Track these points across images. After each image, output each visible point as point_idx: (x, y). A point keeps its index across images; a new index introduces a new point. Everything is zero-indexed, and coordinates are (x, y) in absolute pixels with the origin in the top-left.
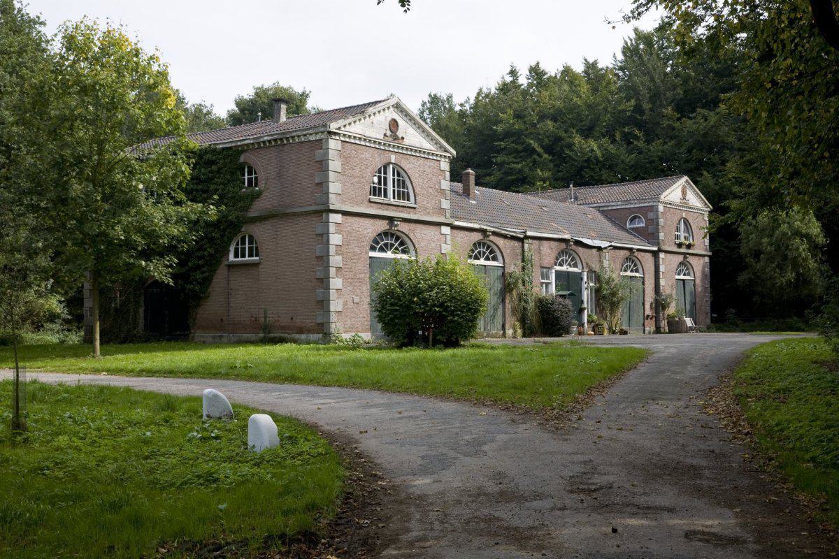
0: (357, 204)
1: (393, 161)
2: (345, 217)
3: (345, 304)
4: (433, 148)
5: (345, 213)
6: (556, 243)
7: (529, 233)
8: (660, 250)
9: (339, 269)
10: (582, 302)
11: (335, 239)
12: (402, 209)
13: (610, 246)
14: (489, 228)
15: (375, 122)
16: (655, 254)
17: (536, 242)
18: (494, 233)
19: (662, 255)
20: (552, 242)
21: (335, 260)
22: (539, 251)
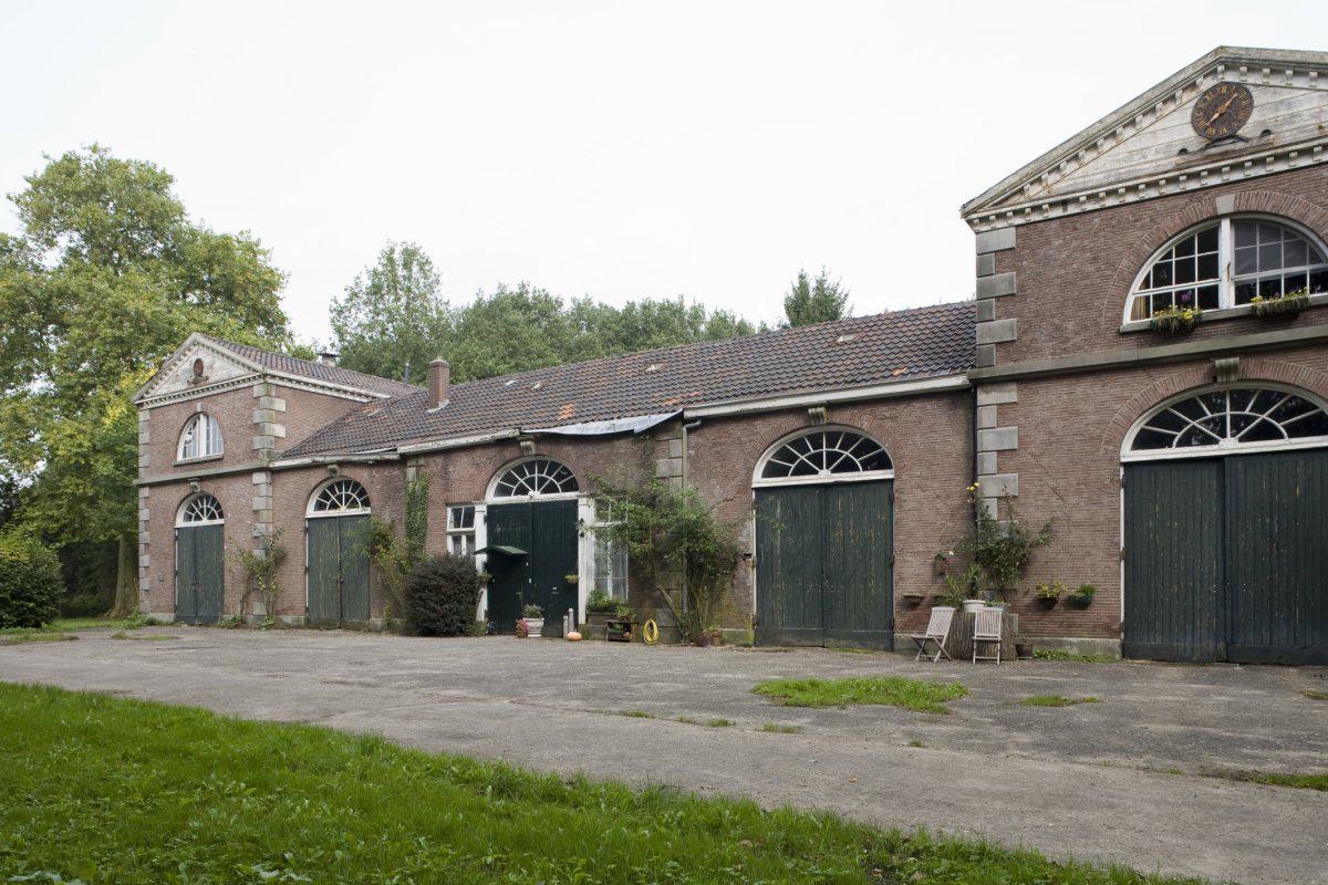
0: (163, 472)
1: (199, 410)
2: (154, 490)
3: (151, 582)
4: (243, 372)
5: (152, 485)
6: (492, 452)
7: (402, 449)
8: (977, 384)
9: (147, 545)
10: (572, 565)
11: (144, 514)
12: (190, 467)
13: (680, 418)
14: (328, 459)
15: (180, 372)
16: (964, 398)
17: (439, 460)
18: (341, 464)
19: (983, 398)
20: (479, 452)
21: (144, 536)
22: (445, 473)
